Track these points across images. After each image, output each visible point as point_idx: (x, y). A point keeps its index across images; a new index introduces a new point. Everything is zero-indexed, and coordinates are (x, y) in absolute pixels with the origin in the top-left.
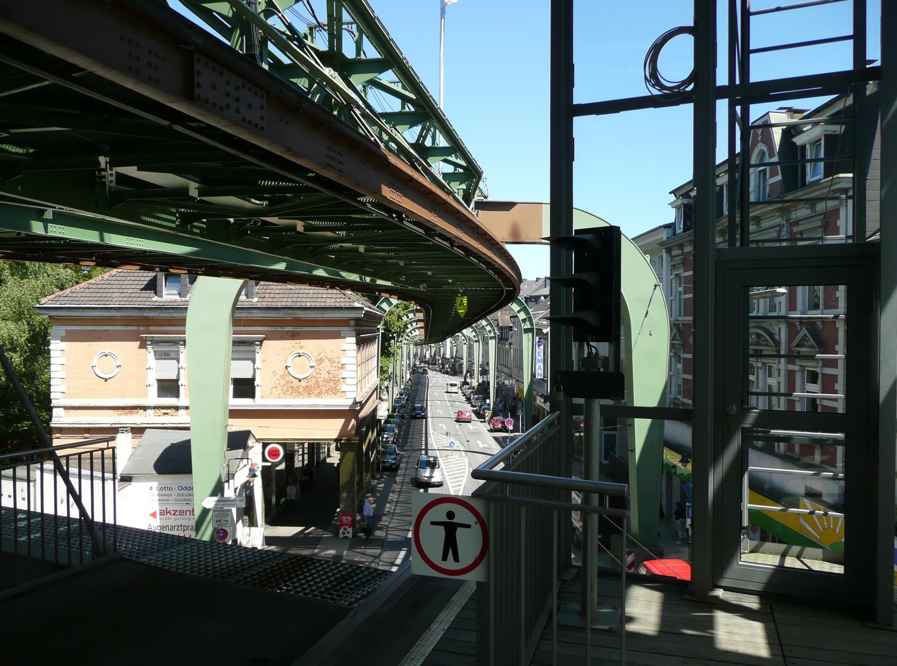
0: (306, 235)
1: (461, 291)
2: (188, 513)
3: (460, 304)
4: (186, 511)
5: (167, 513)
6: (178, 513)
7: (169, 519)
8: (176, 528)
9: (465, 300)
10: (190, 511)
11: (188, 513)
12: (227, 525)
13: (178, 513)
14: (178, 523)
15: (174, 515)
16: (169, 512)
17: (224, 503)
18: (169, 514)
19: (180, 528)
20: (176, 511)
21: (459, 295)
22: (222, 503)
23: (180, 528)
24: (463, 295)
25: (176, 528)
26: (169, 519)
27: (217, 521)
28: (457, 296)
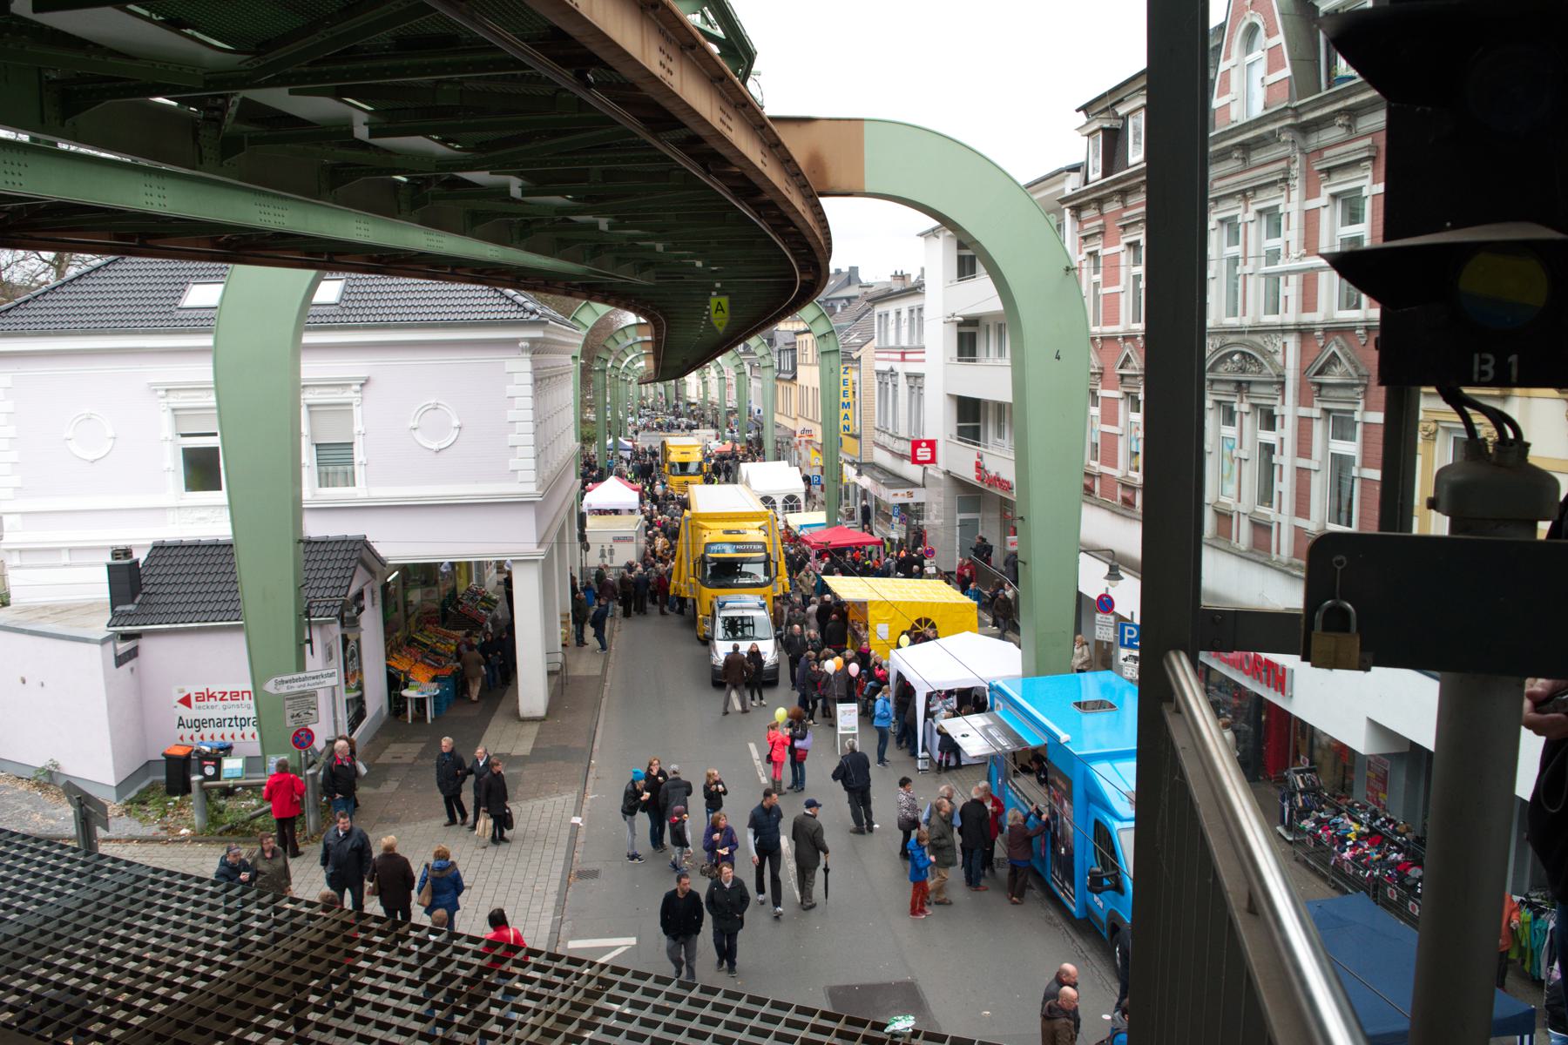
0: (387, 151)
2: (246, 695)
3: (717, 310)
4: (243, 692)
5: (209, 697)
6: (228, 696)
7: (213, 707)
8: (227, 722)
9: (724, 301)
10: (249, 692)
11: (246, 695)
12: (311, 721)
13: (228, 696)
14: (230, 713)
15: (221, 699)
16: (212, 696)
17: (302, 683)
18: (212, 699)
19: (233, 723)
20: (225, 693)
21: (714, 293)
22: (299, 683)
23: (233, 723)
24: (721, 293)
25: (227, 722)
26: (213, 707)
27: (293, 717)
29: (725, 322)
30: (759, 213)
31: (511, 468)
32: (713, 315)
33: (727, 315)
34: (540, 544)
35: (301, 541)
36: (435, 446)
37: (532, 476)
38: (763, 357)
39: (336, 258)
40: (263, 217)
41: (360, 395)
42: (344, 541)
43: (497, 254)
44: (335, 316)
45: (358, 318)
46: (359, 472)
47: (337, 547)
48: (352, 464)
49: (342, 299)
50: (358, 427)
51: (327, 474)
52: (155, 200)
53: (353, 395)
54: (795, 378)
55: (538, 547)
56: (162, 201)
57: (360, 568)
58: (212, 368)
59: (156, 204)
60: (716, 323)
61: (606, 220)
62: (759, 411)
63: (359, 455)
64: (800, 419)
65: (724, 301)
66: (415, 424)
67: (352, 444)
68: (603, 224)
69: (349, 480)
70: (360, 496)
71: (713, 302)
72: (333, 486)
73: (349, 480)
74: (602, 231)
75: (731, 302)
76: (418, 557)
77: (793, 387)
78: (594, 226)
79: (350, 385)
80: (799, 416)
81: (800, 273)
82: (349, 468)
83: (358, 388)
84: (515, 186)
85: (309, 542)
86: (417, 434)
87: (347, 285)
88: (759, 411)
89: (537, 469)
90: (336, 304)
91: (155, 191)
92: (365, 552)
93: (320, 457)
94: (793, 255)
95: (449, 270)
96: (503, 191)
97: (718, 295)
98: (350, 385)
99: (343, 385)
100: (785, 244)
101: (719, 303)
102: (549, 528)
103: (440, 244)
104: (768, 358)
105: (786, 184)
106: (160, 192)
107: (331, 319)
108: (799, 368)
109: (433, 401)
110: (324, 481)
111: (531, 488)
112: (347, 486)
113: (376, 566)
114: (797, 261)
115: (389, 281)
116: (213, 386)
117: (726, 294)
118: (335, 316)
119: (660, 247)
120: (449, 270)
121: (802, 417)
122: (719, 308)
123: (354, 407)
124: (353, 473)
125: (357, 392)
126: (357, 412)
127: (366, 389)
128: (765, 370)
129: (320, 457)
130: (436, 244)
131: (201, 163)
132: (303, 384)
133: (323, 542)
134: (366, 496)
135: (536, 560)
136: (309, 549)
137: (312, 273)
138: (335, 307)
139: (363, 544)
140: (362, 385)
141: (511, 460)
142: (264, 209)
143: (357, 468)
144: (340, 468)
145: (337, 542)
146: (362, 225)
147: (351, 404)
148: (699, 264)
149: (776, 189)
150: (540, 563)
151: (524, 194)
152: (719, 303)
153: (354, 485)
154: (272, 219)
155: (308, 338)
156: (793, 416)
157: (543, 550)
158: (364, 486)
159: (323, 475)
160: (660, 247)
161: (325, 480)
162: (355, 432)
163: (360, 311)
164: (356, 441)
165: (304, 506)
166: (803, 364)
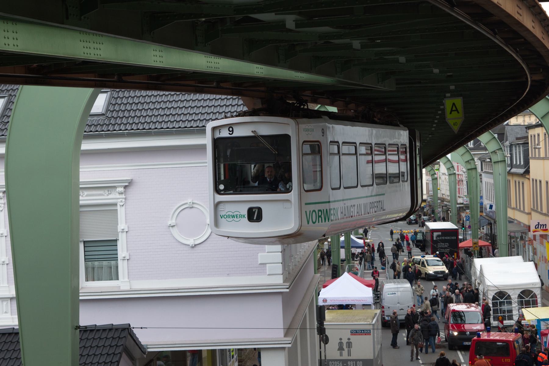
1: (452, 87)
3: (452, 111)
9: (459, 102)
21: (448, 95)
24: (454, 95)
28: (445, 97)
29: (459, 122)
30: (493, 30)
31: (259, 263)
32: (448, 116)
33: (461, 115)
34: (288, 331)
35: (78, 327)
36: (191, 242)
37: (279, 269)
38: (494, 152)
39: (125, 78)
40: (86, 50)
41: (123, 196)
42: (110, 330)
43: (262, 71)
44: (96, 126)
45: (123, 127)
46: (122, 266)
47: (104, 335)
48: (116, 259)
49: (107, 110)
50: (122, 225)
51: (93, 268)
52: (11, 42)
53: (118, 196)
54: (527, 172)
55: (286, 335)
56: (15, 42)
57: (124, 355)
58: (4, 173)
59: (11, 45)
60: (451, 122)
61: (359, 41)
62: (491, 207)
63: (122, 252)
64: (533, 213)
65: (459, 102)
66: (172, 222)
67: (116, 241)
68: (356, 44)
69: (113, 275)
70: (122, 288)
71: (448, 103)
72: (99, 280)
73: (113, 275)
74: (354, 49)
75: (464, 103)
76: (174, 345)
77: (526, 182)
78: (349, 47)
79: (115, 187)
80: (532, 210)
81: (531, 74)
82: (113, 263)
83: (121, 189)
84: (290, 21)
85: (86, 330)
86: (175, 231)
87: (112, 97)
88: (491, 207)
89: (284, 263)
90: (103, 115)
91: (11, 35)
92: (129, 343)
93: (87, 253)
94: (523, 60)
95: (215, 84)
96: (280, 26)
97: (453, 96)
98: (115, 187)
99: (109, 187)
100: (517, 52)
101: (454, 104)
102: (294, 318)
103: (217, 65)
104: (499, 153)
105: (517, 9)
106: (15, 35)
107: (99, 128)
108: (532, 163)
109: (189, 201)
110: (90, 276)
111: (279, 280)
112: (111, 279)
113: (137, 354)
114: (527, 65)
115: (181, 97)
116: (5, 187)
117: (461, 95)
118: (96, 126)
119: (402, 59)
120: (215, 84)
121: (536, 211)
122: (454, 108)
123: (118, 207)
124: (117, 267)
125: (121, 193)
126: (121, 212)
127: (130, 190)
128: (497, 165)
129: (87, 253)
130: (212, 65)
131: (67, 18)
132: (81, 186)
133: (92, 331)
134: (127, 288)
135: (284, 348)
136: (85, 336)
137: (90, 90)
138: (101, 118)
139: (127, 330)
140: (125, 187)
141: (259, 254)
142: (86, 44)
143: (120, 263)
144: (105, 263)
145: (104, 330)
146: (158, 53)
147: (115, 205)
148: (436, 71)
149: (509, 16)
150: (287, 349)
151: (297, 26)
152: (454, 104)
153: (118, 279)
154: (92, 51)
155: (86, 146)
156: (526, 211)
157: (289, 339)
158: (127, 279)
159: (90, 270)
160: (402, 59)
161: (92, 276)
162: (119, 230)
163: (124, 121)
164: (120, 238)
165: (81, 298)
166: (535, 158)
